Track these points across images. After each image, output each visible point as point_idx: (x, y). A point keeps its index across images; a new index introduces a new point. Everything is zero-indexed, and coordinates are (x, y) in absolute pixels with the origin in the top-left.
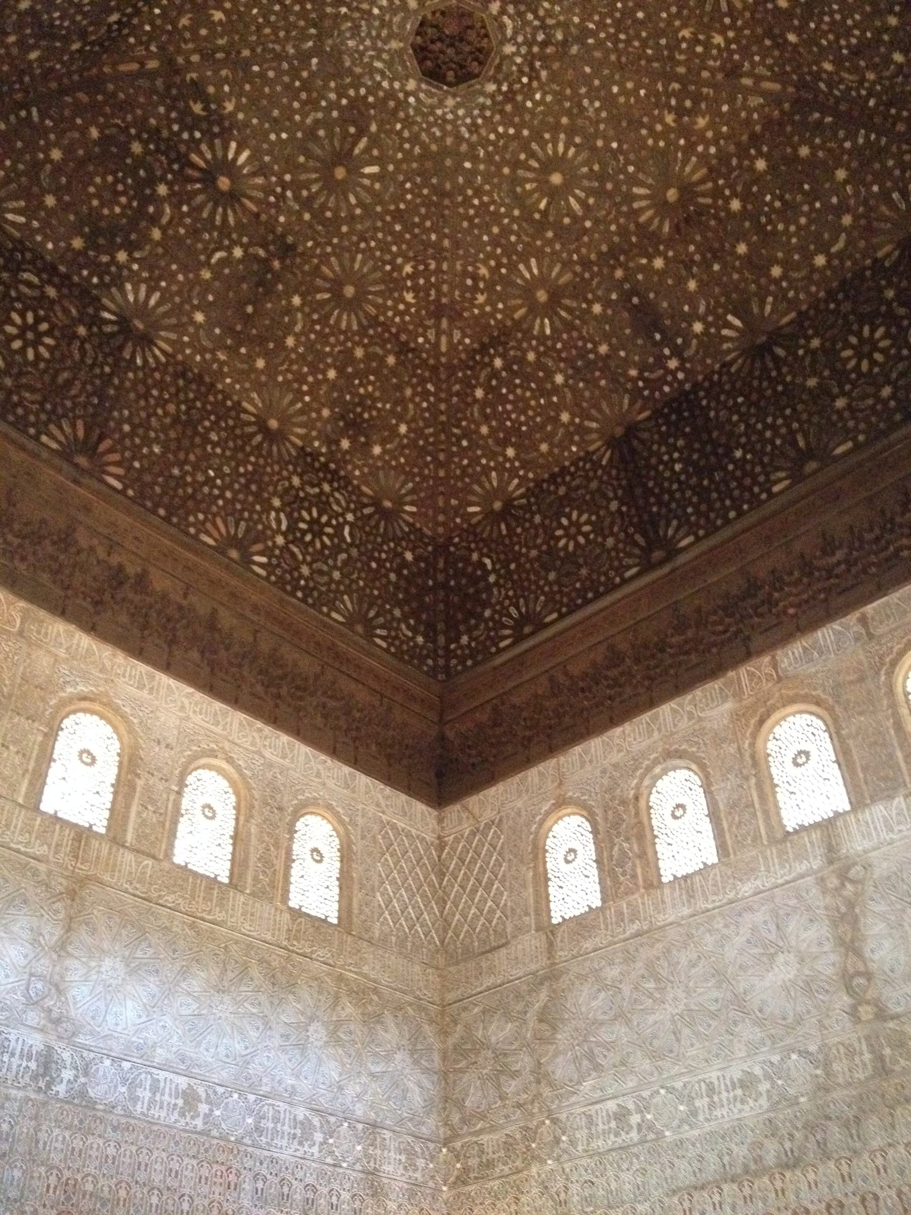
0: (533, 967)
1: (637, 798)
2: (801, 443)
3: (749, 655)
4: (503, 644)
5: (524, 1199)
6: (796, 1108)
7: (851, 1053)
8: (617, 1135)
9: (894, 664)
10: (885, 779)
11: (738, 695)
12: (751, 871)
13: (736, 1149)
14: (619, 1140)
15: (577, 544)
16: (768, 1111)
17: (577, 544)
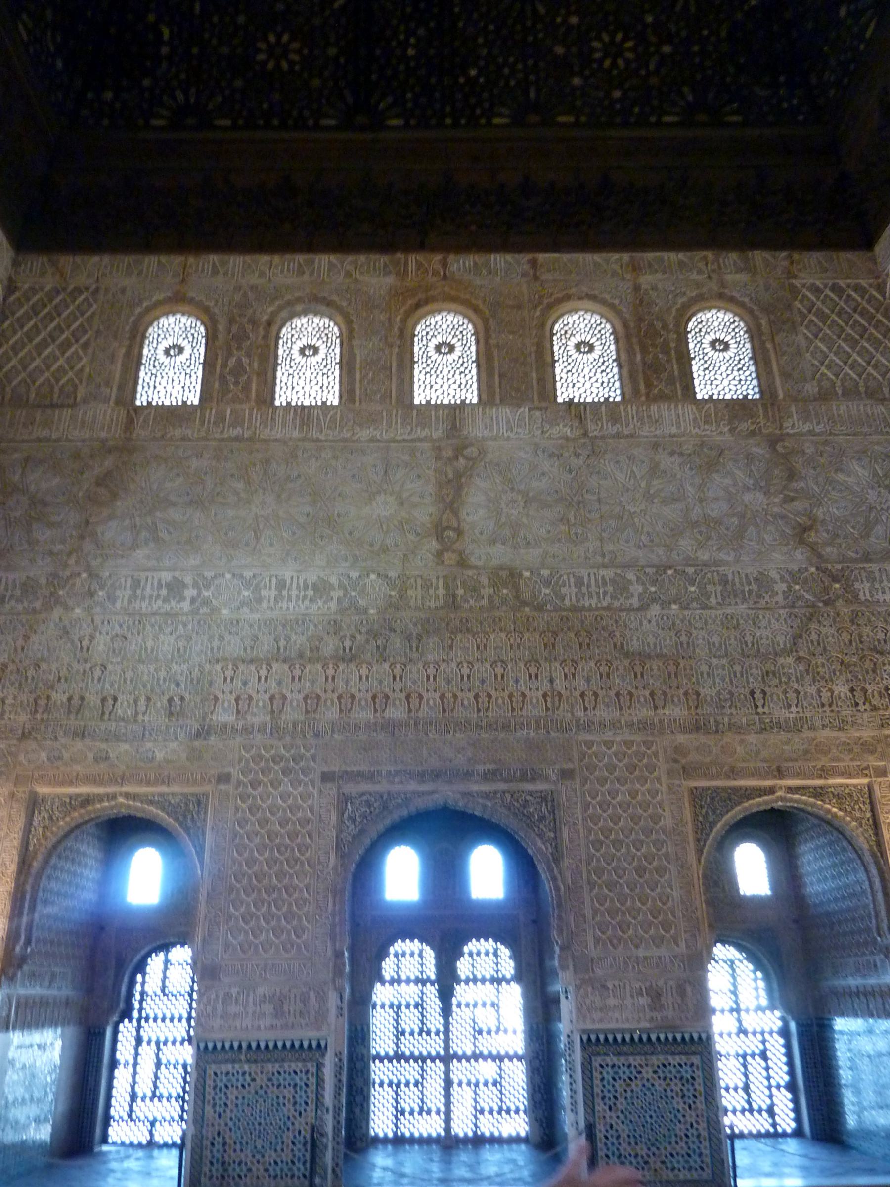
0: (103, 435)
1: (269, 324)
2: (532, 95)
3: (421, 247)
4: (156, 122)
5: (35, 638)
6: (364, 617)
7: (427, 585)
8: (166, 600)
9: (550, 306)
10: (518, 390)
11: (402, 275)
12: (373, 420)
13: (294, 637)
14: (167, 607)
15: (278, 66)
16: (336, 613)
17: (278, 66)
